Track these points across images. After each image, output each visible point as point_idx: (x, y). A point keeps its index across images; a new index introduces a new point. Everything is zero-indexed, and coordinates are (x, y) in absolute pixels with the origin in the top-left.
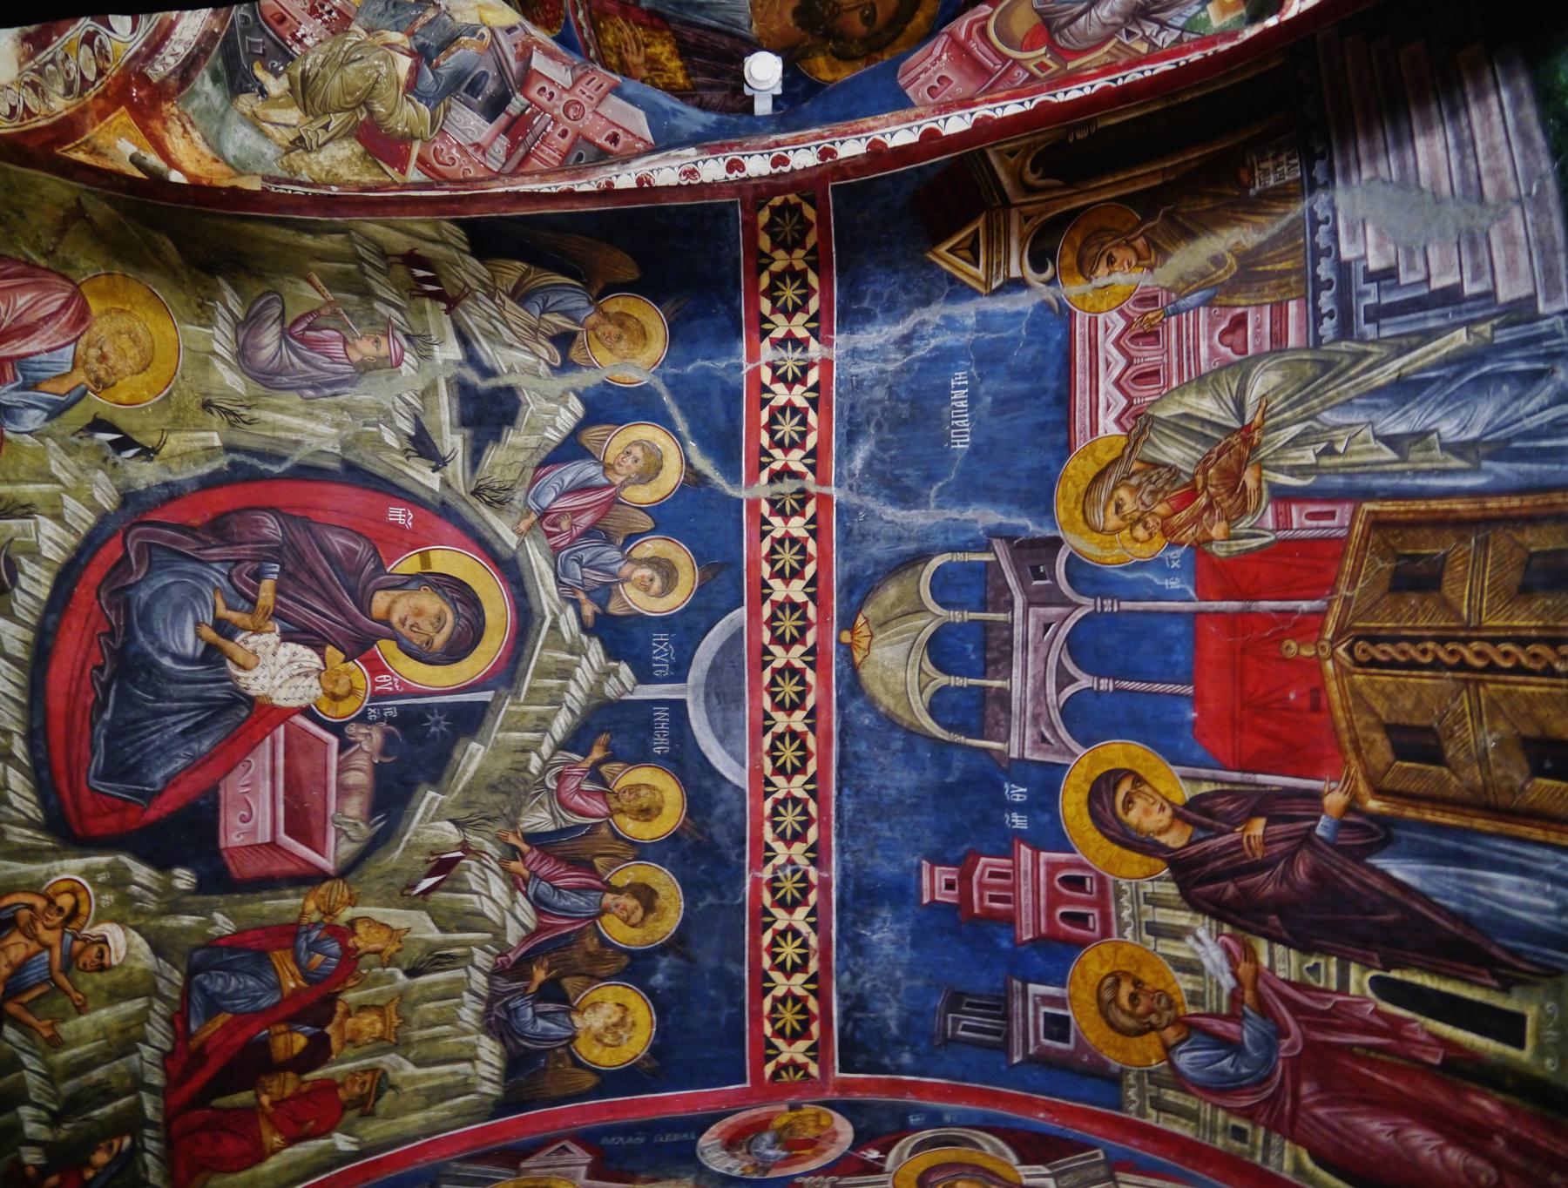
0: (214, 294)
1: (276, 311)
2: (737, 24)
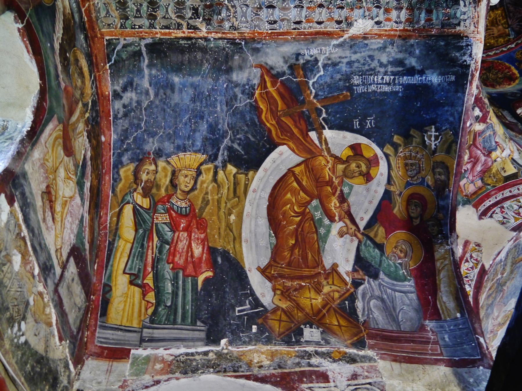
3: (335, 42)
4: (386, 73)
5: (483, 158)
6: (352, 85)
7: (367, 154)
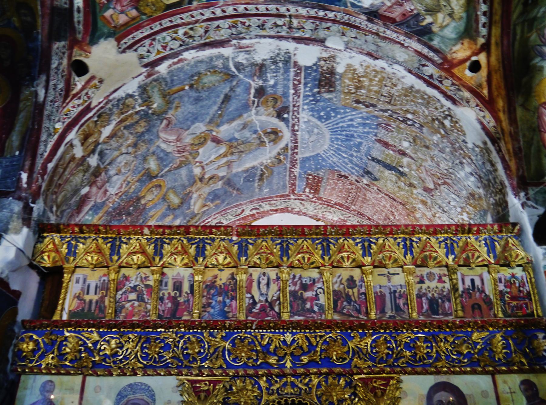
0: (535, 66)
1: (538, 47)
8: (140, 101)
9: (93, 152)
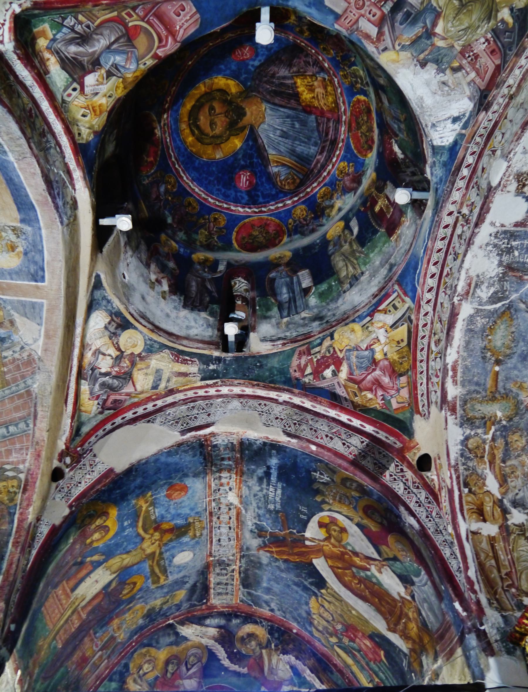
2: (271, 109)
3: (244, 512)
4: (268, 490)
5: (378, 372)
6: (274, 510)
7: (327, 521)
8: (480, 431)
9: (505, 512)
